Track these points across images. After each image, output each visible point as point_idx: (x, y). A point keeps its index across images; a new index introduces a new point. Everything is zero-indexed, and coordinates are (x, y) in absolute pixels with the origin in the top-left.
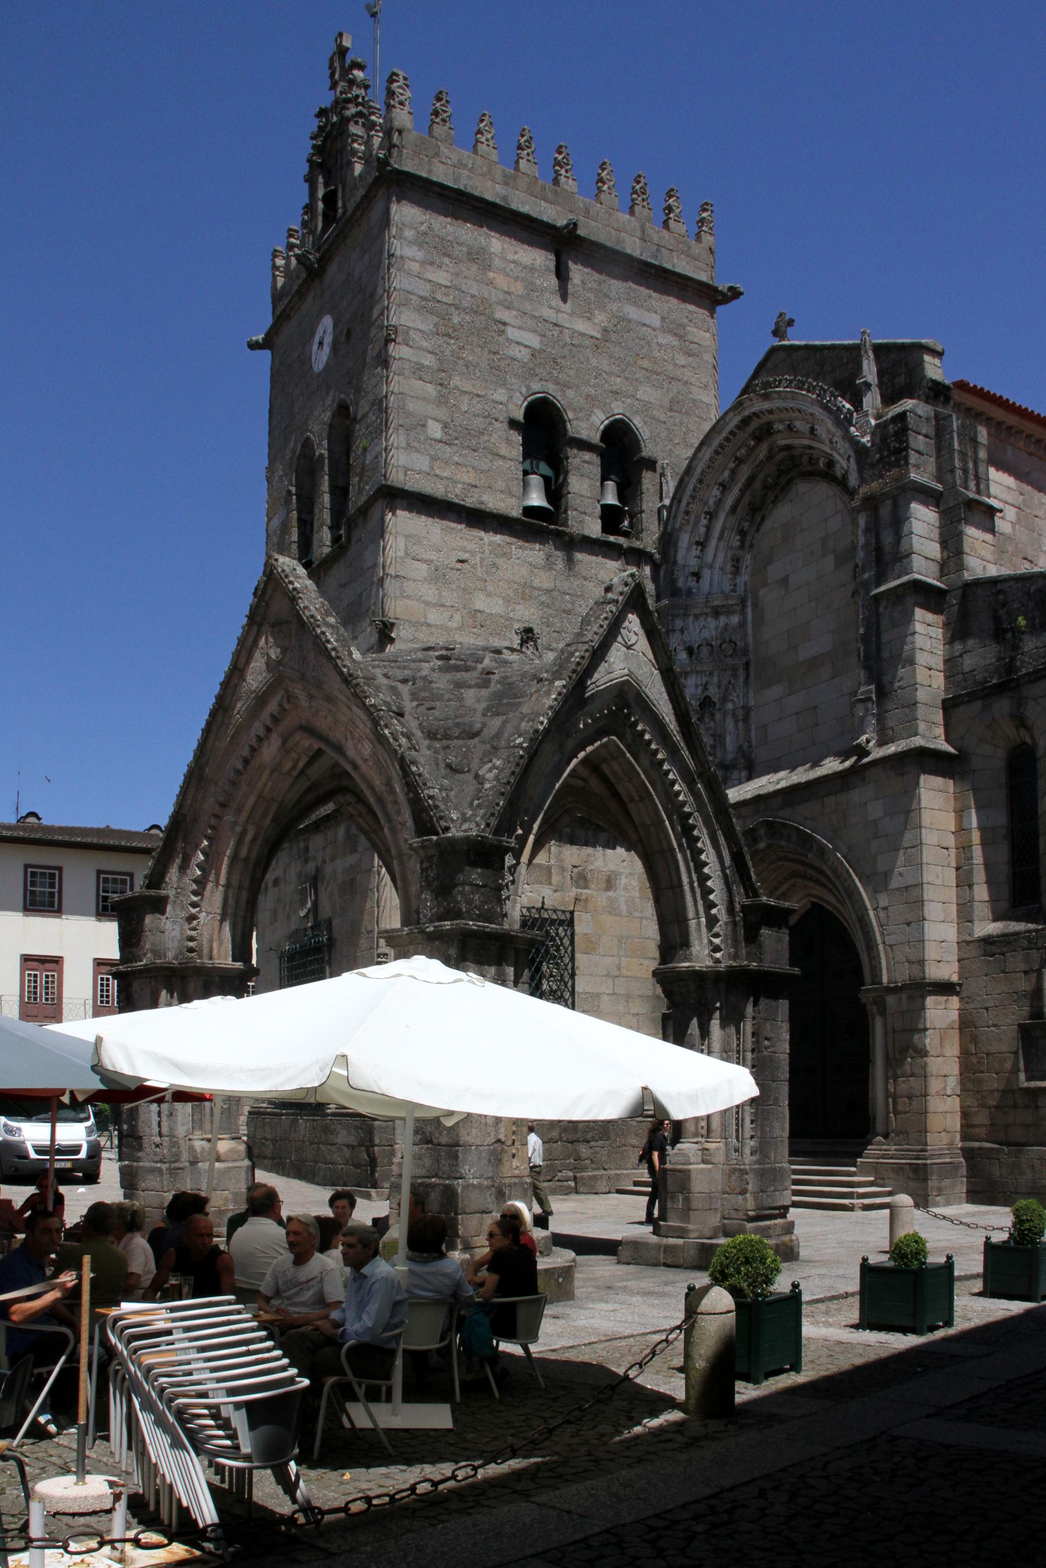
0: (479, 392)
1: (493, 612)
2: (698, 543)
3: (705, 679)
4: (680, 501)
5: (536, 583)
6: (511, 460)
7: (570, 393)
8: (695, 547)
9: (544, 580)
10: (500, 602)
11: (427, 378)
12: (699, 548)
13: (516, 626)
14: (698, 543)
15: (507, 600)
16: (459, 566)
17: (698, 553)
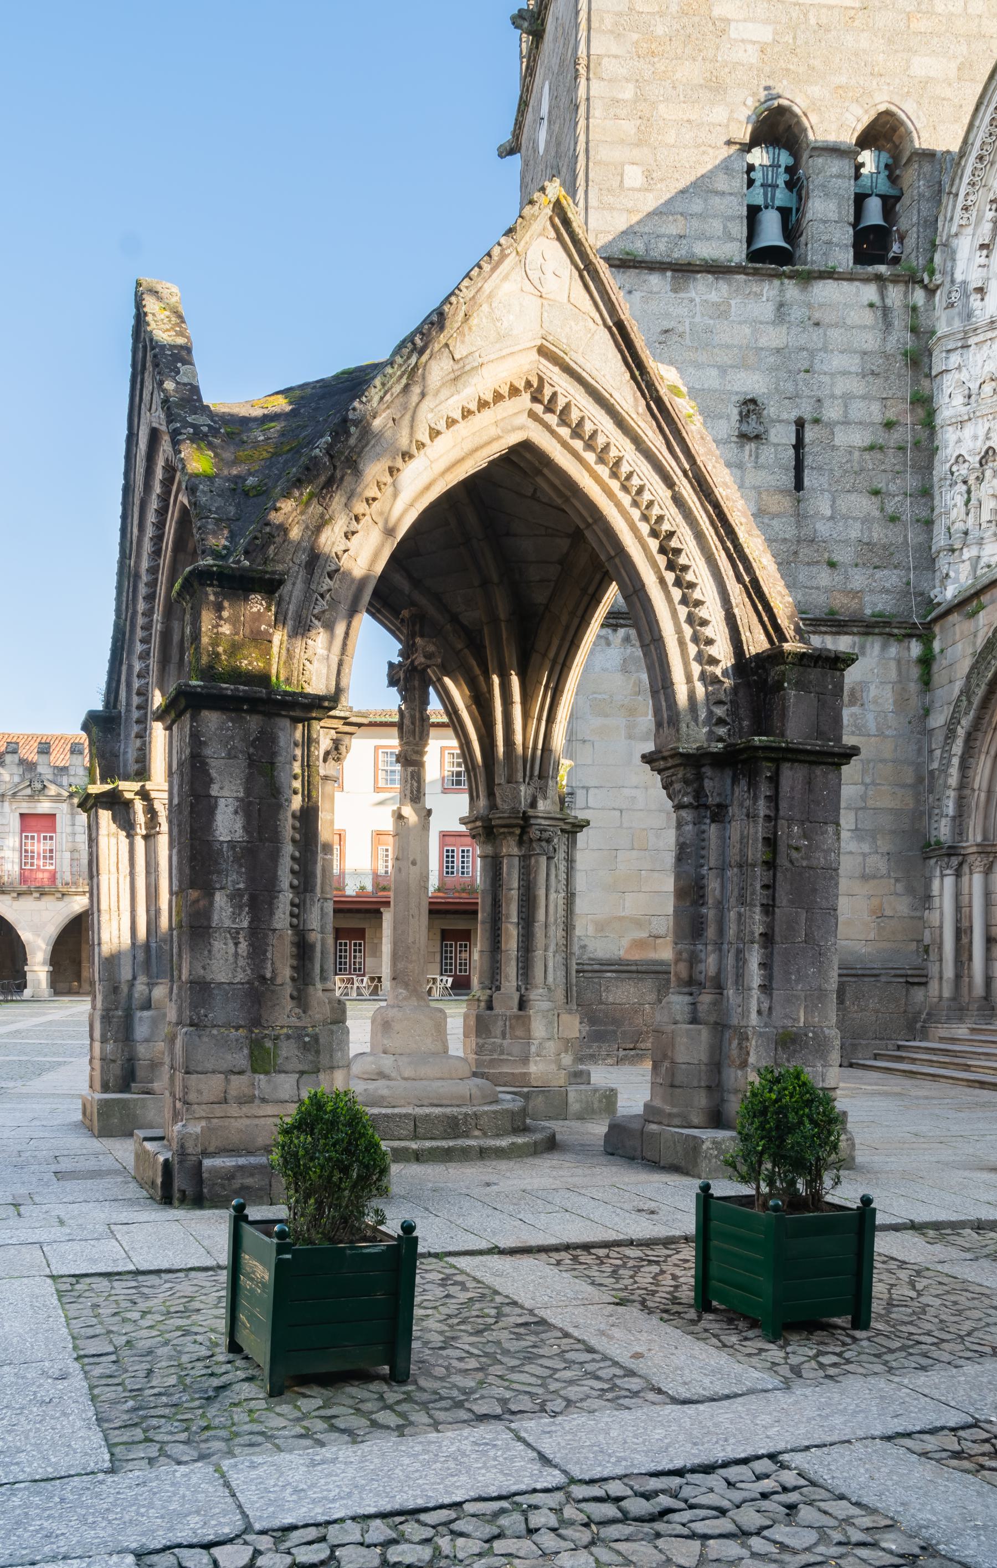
0: (692, 117)
1: (706, 386)
2: (982, 247)
3: (987, 425)
4: (957, 195)
5: (763, 342)
6: (731, 194)
7: (815, 91)
8: (978, 253)
9: (774, 337)
10: (714, 372)
11: (623, 113)
12: (985, 252)
13: (735, 398)
14: (982, 247)
15: (723, 370)
16: (662, 338)
17: (983, 261)
